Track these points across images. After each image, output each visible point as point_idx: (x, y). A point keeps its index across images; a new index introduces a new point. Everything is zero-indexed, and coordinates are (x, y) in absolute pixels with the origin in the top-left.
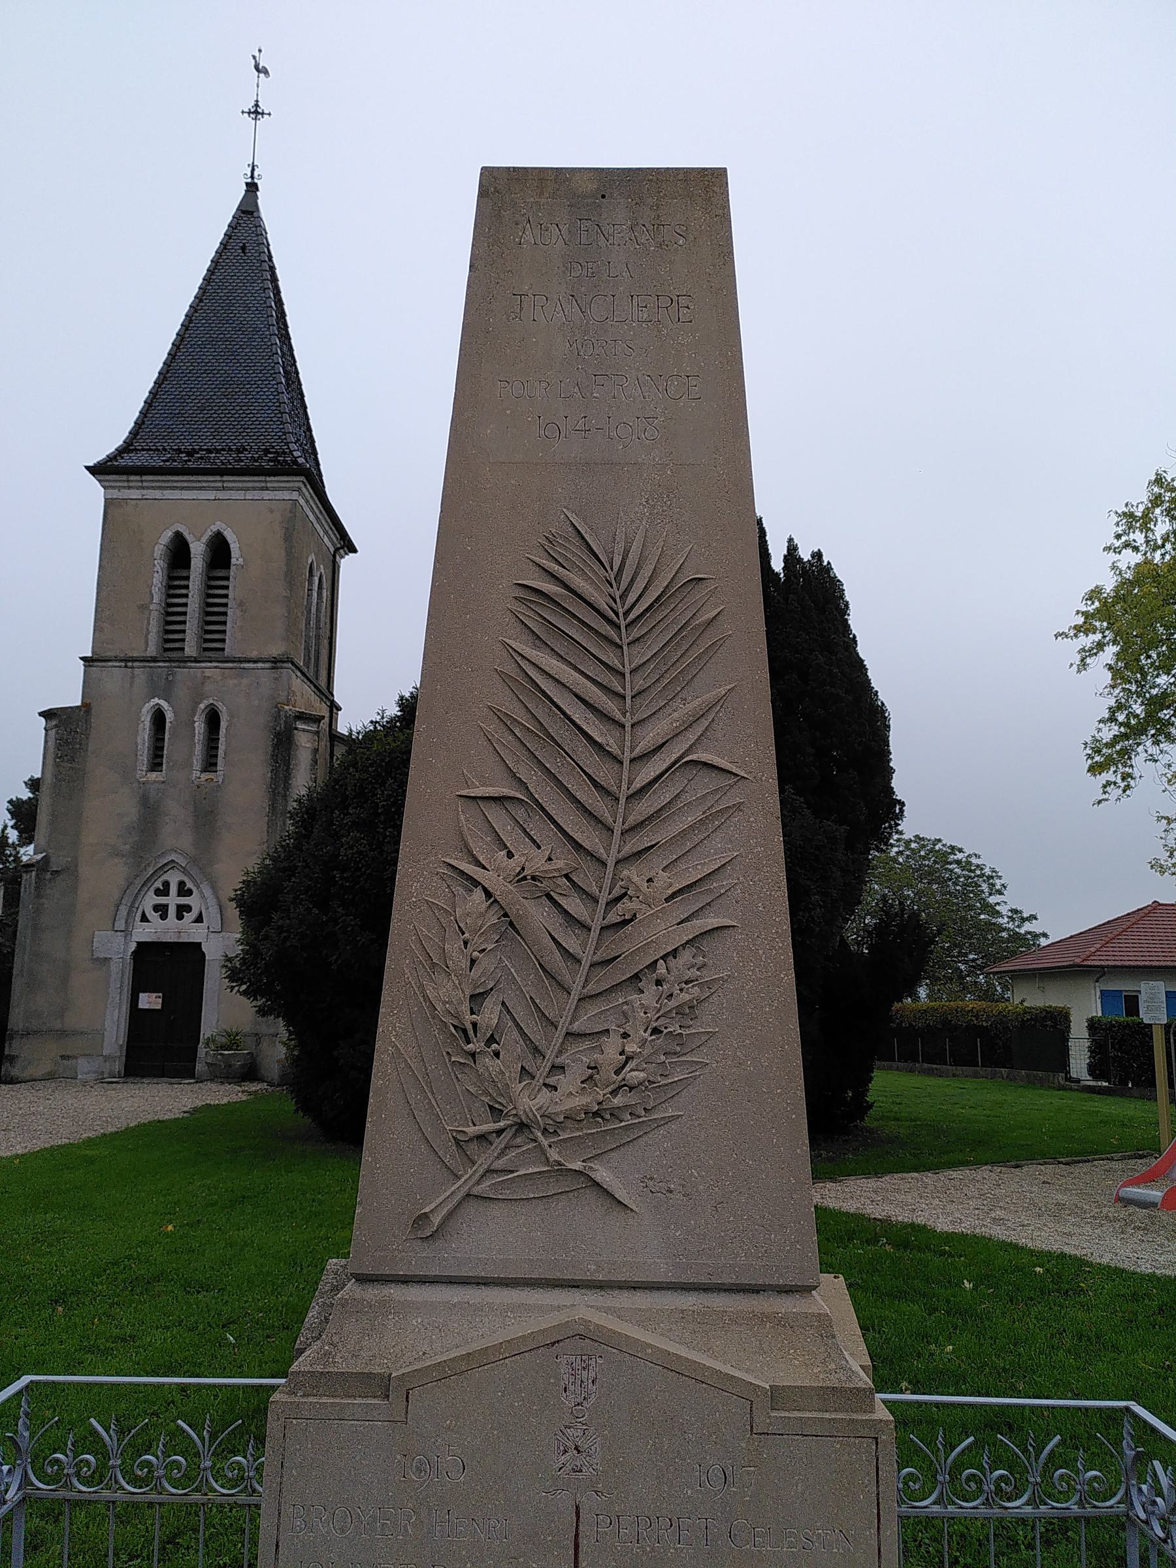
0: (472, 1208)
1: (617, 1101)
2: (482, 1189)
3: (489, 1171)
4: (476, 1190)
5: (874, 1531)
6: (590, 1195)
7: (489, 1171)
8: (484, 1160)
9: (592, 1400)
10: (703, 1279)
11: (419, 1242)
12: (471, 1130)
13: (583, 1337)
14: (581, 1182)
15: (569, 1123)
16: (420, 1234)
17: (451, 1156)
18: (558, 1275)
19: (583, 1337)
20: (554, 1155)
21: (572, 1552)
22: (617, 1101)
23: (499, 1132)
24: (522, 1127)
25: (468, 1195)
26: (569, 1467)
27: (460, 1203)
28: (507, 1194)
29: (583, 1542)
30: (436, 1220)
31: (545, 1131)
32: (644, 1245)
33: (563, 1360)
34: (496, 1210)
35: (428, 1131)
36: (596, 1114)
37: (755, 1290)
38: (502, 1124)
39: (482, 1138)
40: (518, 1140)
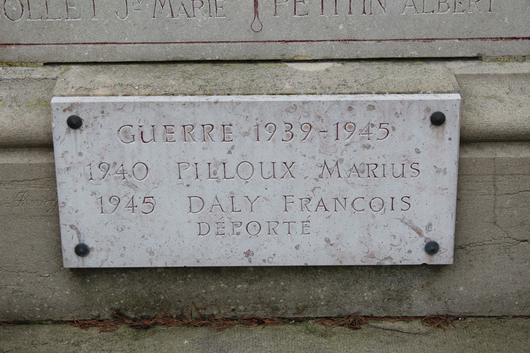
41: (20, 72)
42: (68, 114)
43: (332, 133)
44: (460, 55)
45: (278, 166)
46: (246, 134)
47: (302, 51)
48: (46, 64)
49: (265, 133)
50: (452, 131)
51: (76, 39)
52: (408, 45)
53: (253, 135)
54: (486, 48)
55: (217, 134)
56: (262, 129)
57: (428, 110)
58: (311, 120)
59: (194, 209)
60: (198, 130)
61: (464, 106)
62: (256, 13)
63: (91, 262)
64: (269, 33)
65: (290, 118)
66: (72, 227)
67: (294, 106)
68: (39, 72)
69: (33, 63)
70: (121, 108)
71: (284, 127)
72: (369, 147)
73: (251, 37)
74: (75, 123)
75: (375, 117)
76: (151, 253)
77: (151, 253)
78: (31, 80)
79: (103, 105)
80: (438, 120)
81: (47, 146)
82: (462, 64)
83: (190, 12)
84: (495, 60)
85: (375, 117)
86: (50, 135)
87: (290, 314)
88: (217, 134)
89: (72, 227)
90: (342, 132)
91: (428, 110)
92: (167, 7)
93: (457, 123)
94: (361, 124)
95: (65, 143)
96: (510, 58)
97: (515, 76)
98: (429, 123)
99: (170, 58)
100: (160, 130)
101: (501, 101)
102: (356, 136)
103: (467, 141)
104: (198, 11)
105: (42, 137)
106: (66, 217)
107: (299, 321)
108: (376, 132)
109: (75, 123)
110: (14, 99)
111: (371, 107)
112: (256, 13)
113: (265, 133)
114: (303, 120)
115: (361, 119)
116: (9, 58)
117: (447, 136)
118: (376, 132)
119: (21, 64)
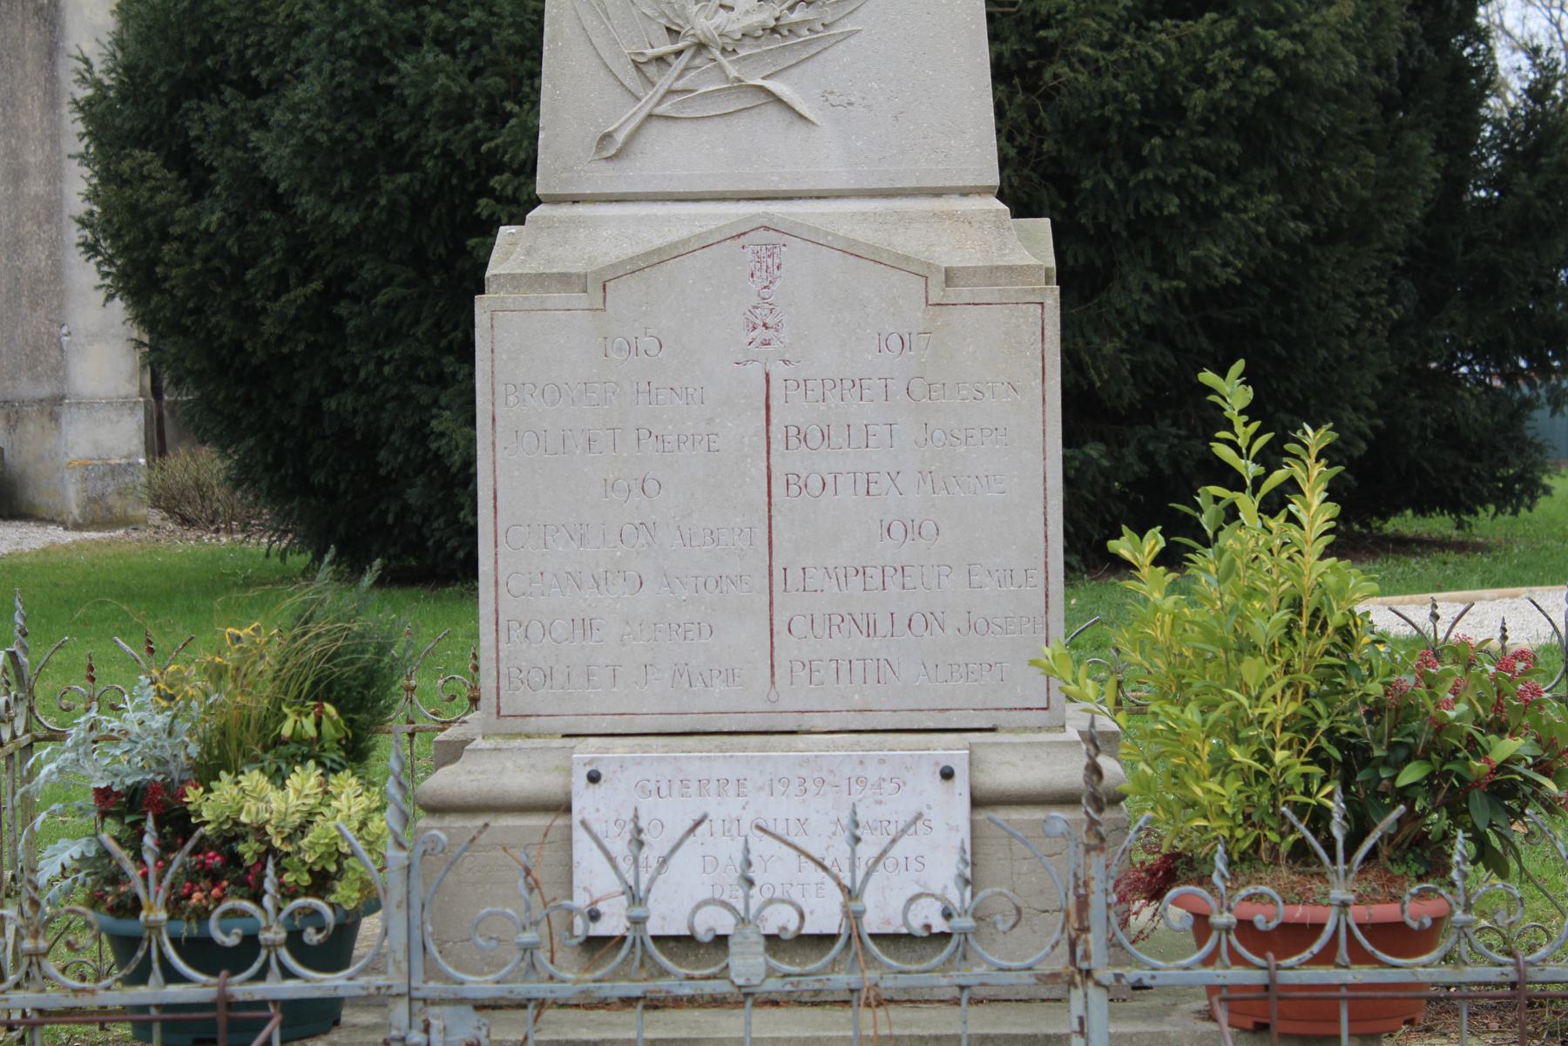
0: (655, 128)
1: (796, 16)
2: (663, 109)
3: (670, 92)
4: (659, 110)
5: (1039, 381)
6: (772, 112)
7: (670, 92)
8: (666, 80)
9: (778, 283)
10: (885, 185)
11: (603, 163)
12: (650, 52)
13: (767, 228)
14: (762, 99)
15: (747, 41)
16: (606, 154)
17: (630, 78)
18: (742, 187)
19: (767, 228)
20: (733, 72)
21: (763, 412)
22: (796, 16)
23: (679, 53)
24: (701, 47)
25: (650, 116)
26: (758, 341)
27: (639, 128)
28: (688, 113)
29: (773, 403)
30: (620, 138)
31: (724, 50)
32: (823, 156)
33: (749, 250)
34: (676, 129)
35: (606, 55)
36: (774, 30)
37: (937, 193)
38: (680, 45)
39: (660, 59)
40: (697, 62)
41: (538, 742)
42: (589, 769)
43: (845, 788)
44: (976, 725)
45: (792, 822)
46: (760, 789)
47: (819, 722)
48: (565, 736)
49: (779, 788)
50: (961, 785)
51: (596, 710)
52: (923, 715)
53: (767, 789)
54: (1000, 718)
55: (732, 788)
56: (775, 783)
57: (937, 764)
58: (824, 774)
59: (709, 869)
60: (714, 784)
61: (972, 762)
62: (773, 683)
63: (599, 929)
64: (785, 704)
65: (803, 773)
66: (585, 889)
67: (808, 760)
68: (559, 742)
69: (552, 735)
70: (639, 762)
71: (797, 781)
72: (880, 802)
73: (767, 707)
74: (594, 778)
75: (886, 771)
76: (664, 919)
77: (664, 919)
78: (550, 749)
79: (622, 760)
80: (947, 774)
81: (565, 808)
82: (978, 735)
83: (708, 681)
84: (1011, 731)
85: (886, 771)
86: (568, 795)
87: (806, 998)
88: (732, 788)
89: (585, 889)
90: (854, 787)
91: (937, 764)
92: (685, 676)
93: (966, 777)
94: (873, 778)
95: (585, 801)
96: (1026, 729)
97: (1030, 744)
98: (938, 777)
99: (687, 729)
100: (676, 785)
101: (1014, 765)
102: (868, 791)
103: (977, 802)
104: (716, 682)
105: (561, 797)
106: (579, 878)
107: (814, 1004)
108: (889, 787)
109: (594, 778)
110: (533, 766)
111: (882, 761)
112: (773, 683)
113: (779, 788)
114: (816, 775)
115: (872, 773)
116: (528, 729)
117: (957, 791)
118: (889, 787)
119: (540, 735)
